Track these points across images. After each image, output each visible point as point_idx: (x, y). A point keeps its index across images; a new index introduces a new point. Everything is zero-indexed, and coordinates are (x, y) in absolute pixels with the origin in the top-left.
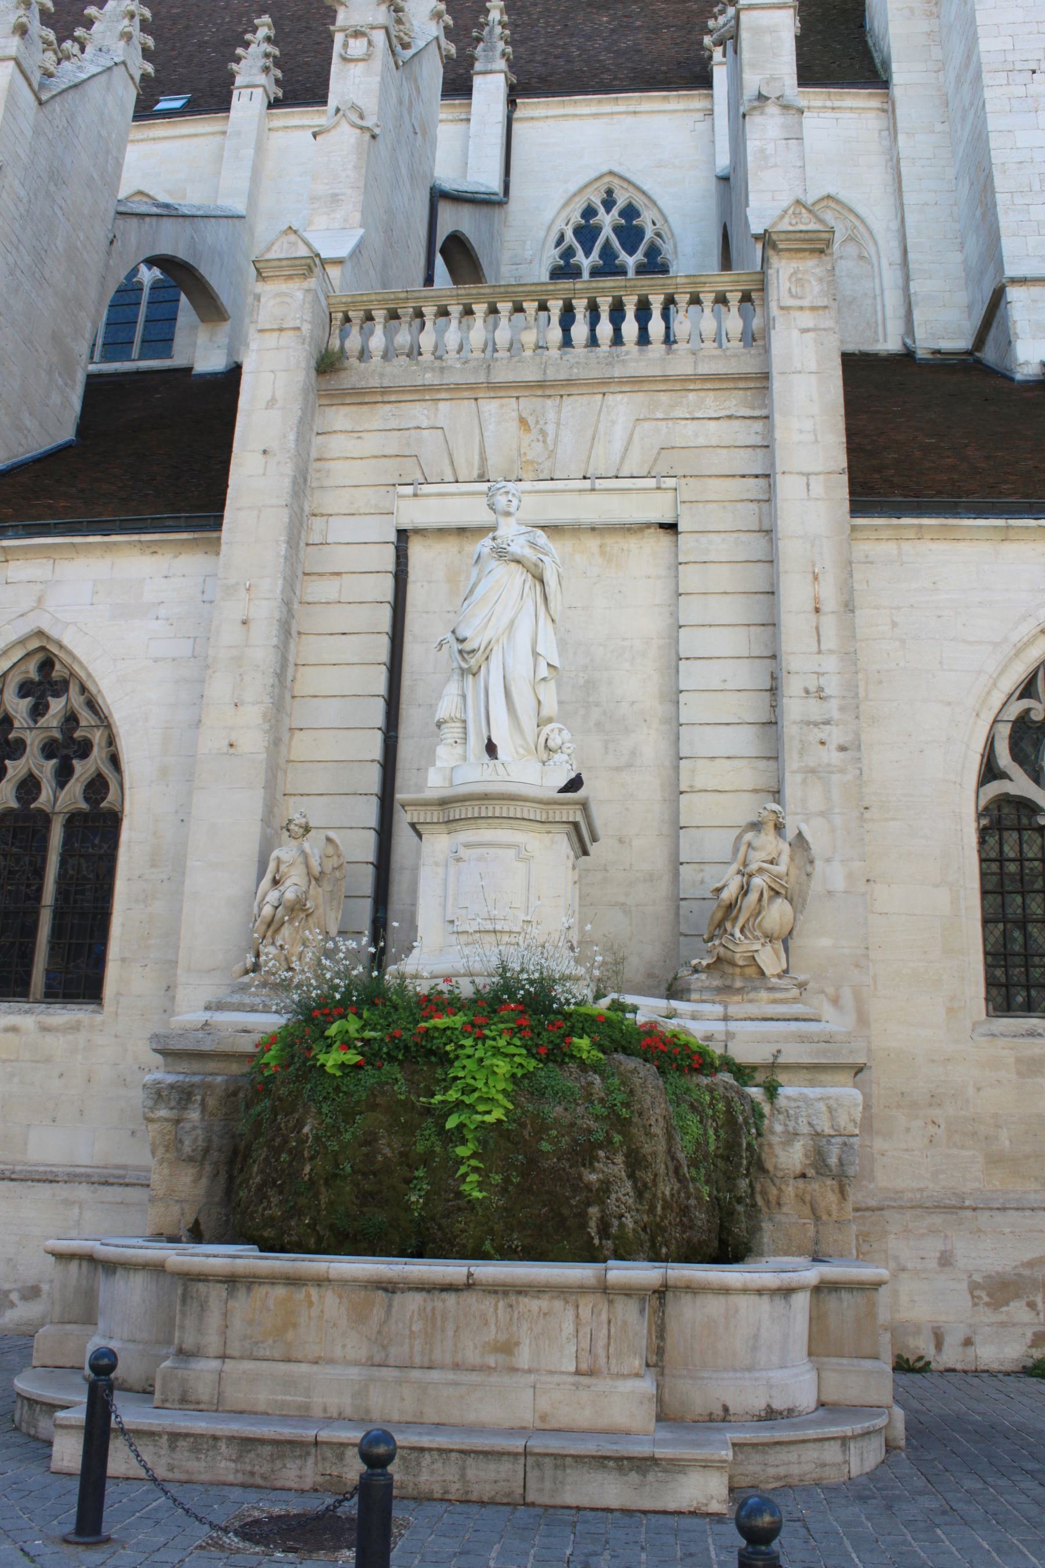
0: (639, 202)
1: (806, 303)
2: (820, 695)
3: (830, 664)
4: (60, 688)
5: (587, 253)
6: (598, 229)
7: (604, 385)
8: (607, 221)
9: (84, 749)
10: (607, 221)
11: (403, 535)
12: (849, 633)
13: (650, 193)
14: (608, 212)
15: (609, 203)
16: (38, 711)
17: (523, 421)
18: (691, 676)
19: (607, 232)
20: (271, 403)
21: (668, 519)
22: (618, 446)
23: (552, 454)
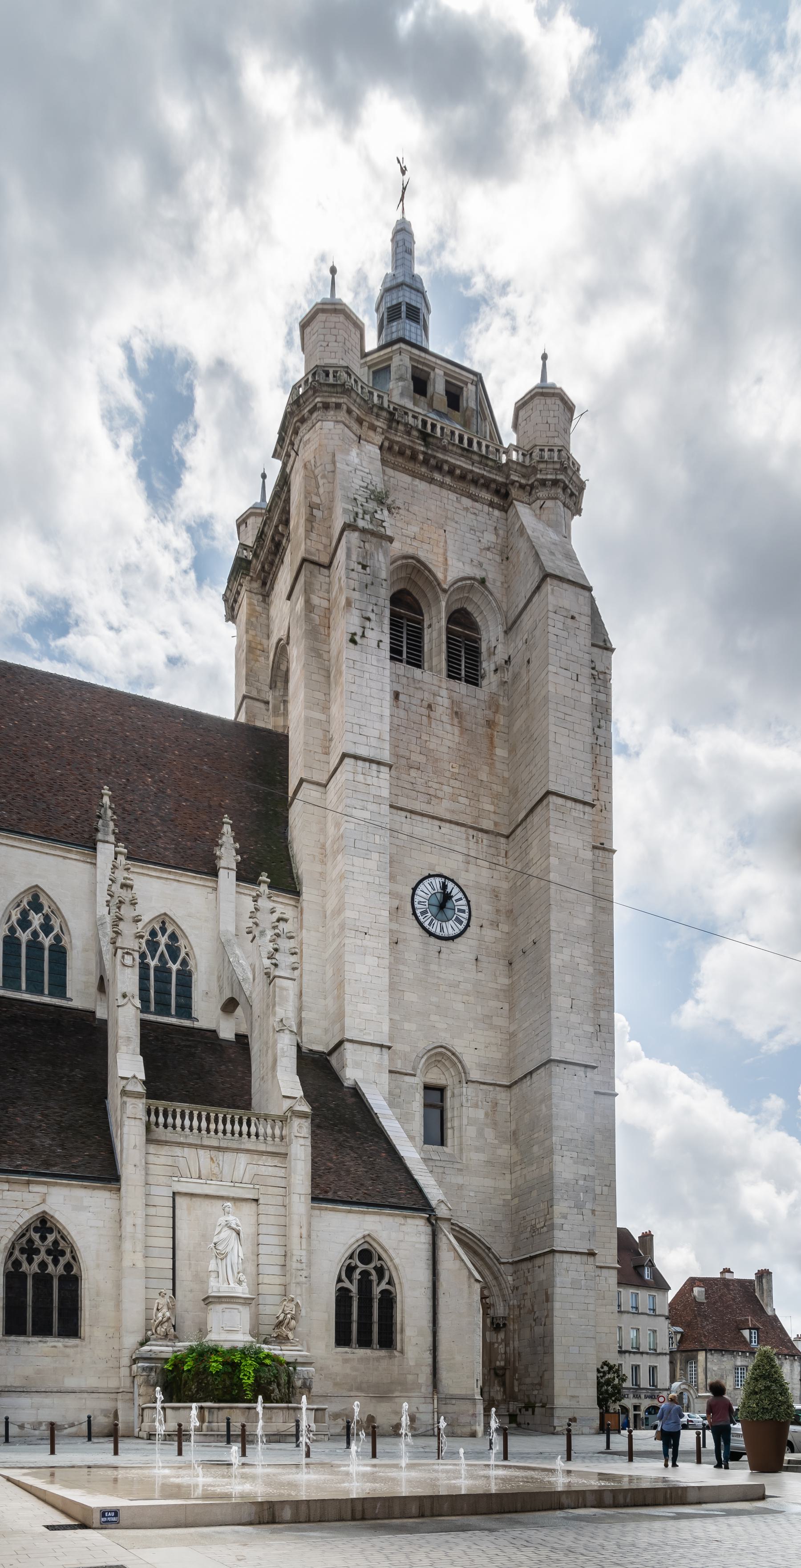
0: (178, 933)
1: (302, 1135)
2: (300, 1262)
3: (304, 1253)
4: (51, 1231)
5: (153, 958)
6: (157, 944)
7: (238, 1150)
8: (163, 940)
9: (63, 1253)
10: (163, 940)
11: (174, 1193)
12: (309, 1244)
13: (185, 931)
14: (163, 936)
15: (163, 930)
16: (43, 1238)
17: (212, 1159)
18: (262, 1249)
19: (162, 948)
20: (135, 1146)
21: (256, 1198)
22: (242, 1172)
23: (221, 1172)
